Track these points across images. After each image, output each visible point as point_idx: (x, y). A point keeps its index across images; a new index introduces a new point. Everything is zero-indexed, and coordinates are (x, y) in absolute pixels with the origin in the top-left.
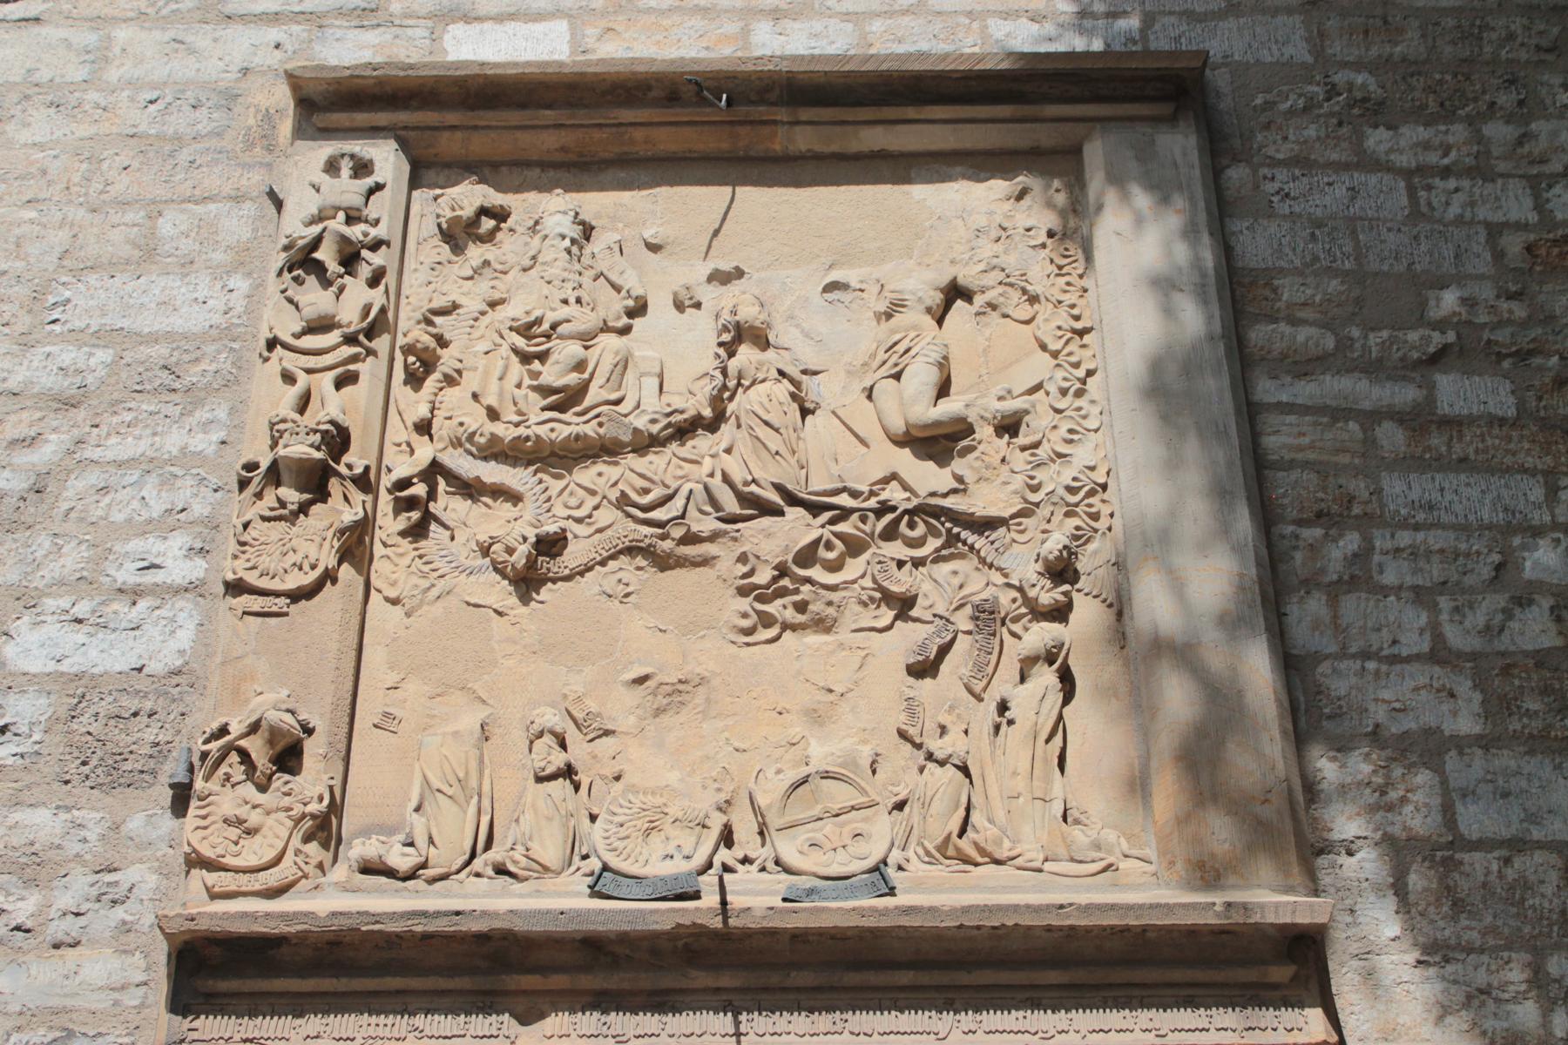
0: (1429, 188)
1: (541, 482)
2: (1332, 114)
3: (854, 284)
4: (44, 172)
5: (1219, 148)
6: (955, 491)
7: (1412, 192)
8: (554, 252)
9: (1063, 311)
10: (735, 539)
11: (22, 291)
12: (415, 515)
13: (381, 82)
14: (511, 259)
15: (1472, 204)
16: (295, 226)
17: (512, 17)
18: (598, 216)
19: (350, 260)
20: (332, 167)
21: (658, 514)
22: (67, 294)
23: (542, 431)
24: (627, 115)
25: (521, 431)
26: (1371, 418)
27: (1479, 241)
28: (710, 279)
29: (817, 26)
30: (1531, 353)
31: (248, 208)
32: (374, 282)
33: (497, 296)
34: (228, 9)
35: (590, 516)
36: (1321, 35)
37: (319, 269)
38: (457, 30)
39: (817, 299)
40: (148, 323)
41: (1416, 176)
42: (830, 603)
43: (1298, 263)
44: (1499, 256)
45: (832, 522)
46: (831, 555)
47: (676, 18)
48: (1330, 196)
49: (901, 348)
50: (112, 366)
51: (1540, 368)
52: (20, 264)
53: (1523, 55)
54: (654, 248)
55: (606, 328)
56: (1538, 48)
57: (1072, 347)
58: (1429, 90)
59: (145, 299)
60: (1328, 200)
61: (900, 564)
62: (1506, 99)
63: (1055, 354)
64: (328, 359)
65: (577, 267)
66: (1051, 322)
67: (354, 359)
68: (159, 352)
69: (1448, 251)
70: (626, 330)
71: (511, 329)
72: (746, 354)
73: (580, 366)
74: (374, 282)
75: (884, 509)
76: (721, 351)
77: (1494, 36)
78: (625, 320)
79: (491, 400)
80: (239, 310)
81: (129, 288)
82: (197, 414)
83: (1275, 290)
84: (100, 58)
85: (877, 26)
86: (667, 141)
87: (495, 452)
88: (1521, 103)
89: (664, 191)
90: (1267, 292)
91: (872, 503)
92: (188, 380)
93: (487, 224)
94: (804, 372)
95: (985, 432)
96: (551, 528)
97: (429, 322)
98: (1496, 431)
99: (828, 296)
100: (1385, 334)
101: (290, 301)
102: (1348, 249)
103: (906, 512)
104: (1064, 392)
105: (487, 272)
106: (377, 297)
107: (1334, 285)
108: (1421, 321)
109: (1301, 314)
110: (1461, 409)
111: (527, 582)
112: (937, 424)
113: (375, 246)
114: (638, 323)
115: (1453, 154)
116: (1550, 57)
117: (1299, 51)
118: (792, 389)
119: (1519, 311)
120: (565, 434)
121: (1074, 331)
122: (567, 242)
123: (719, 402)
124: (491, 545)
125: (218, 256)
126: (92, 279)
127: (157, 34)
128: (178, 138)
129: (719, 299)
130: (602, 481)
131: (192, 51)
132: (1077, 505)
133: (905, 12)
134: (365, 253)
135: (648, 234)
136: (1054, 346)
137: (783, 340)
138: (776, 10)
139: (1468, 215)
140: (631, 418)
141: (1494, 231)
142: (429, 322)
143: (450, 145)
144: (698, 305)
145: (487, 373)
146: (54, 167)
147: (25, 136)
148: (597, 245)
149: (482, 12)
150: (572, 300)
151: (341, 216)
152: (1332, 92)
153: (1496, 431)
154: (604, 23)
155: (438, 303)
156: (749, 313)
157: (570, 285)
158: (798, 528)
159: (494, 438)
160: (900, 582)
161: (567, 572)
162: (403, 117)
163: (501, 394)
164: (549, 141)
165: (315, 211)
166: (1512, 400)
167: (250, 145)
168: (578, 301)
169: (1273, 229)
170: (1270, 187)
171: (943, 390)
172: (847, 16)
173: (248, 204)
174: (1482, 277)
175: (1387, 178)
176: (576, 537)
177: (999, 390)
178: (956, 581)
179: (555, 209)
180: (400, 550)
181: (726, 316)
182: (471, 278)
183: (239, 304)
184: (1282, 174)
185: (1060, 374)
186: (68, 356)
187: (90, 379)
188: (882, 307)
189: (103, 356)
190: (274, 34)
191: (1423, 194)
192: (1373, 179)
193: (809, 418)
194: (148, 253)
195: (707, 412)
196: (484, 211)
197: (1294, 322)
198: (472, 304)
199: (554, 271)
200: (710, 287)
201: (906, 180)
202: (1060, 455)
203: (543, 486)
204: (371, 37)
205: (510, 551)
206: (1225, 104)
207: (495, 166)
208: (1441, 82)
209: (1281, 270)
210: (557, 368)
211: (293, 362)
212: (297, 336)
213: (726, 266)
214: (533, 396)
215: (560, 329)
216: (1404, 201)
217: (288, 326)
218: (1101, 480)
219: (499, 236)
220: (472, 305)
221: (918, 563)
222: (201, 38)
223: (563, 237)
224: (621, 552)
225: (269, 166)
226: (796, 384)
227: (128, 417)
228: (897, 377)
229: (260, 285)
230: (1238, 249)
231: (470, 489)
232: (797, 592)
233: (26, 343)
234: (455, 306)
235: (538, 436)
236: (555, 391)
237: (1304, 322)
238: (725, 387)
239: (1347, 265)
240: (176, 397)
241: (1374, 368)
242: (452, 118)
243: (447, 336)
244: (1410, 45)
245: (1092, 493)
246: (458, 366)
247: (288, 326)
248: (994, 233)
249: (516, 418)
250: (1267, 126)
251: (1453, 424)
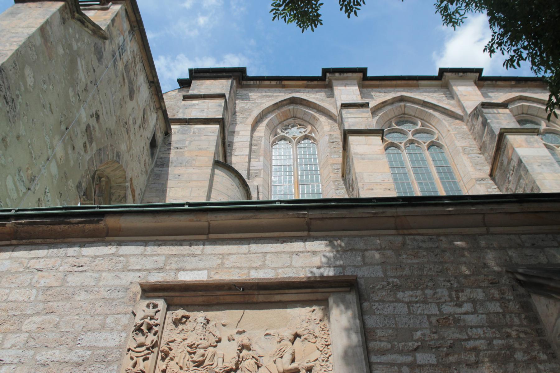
0: (413, 306)
2: (389, 289)
3: (272, 334)
4: (82, 307)
5: (361, 299)
7: (408, 307)
8: (199, 327)
9: (323, 340)
11: (72, 336)
13: (161, 285)
14: (189, 328)
15: (423, 310)
16: (138, 321)
17: (194, 270)
18: (211, 318)
19: (150, 328)
20: (148, 306)
22: (83, 337)
24: (219, 293)
26: (400, 365)
27: (425, 320)
28: (237, 333)
29: (266, 271)
30: (439, 347)
31: (128, 316)
32: (155, 334)
33: (185, 338)
34: (129, 268)
36: (386, 270)
37: (142, 331)
38: (181, 273)
39: (263, 337)
40: (101, 344)
41: (409, 304)
43: (381, 326)
44: (430, 323)
47: (233, 269)
48: (388, 309)
49: (282, 350)
50: (91, 356)
51: (442, 351)
52: (73, 330)
53: (434, 273)
54: (224, 325)
55: (211, 346)
56: (437, 272)
57: (325, 349)
58: (411, 282)
59: (101, 338)
60: (388, 310)
62: (430, 284)
63: (321, 351)
65: (205, 330)
66: (320, 343)
67: (148, 354)
68: (102, 352)
69: (418, 322)
70: (216, 346)
72: (245, 352)
74: (155, 334)
76: (238, 352)
77: (426, 269)
78: (216, 344)
79: (181, 364)
80: (123, 341)
81: (97, 336)
82: (110, 368)
83: (376, 333)
84: (98, 280)
85: (280, 270)
86: (228, 299)
88: (434, 285)
89: (227, 311)
90: (374, 334)
92: (108, 359)
93: (184, 320)
94: (259, 356)
97: (168, 344)
98: (432, 368)
99: (266, 337)
100: (403, 343)
101: (134, 339)
102: (393, 322)
104: (323, 361)
105: (183, 332)
106: (155, 338)
107: (390, 331)
108: (412, 340)
109: (383, 339)
110: (423, 362)
112: (291, 370)
113: (156, 325)
114: (219, 344)
115: (418, 298)
116: (440, 274)
117: (381, 274)
119: (436, 336)
121: (326, 345)
122: (202, 324)
123: (237, 364)
125: (120, 328)
126: (89, 333)
127: (112, 274)
128: (114, 299)
129: (238, 338)
131: (120, 278)
133: (287, 267)
134: (154, 327)
135: (223, 322)
136: (321, 349)
137: (254, 349)
138: (256, 267)
139: (422, 313)
141: (429, 316)
142: (168, 344)
143: (177, 300)
144: (234, 340)
145: (180, 358)
146: (84, 306)
147: (79, 298)
148: (210, 325)
149: (187, 269)
151: (149, 318)
152: (389, 284)
153: (432, 368)
154: (216, 271)
155: (171, 339)
156: (246, 342)
157: (202, 335)
162: (166, 294)
163: (183, 363)
164: (200, 300)
165: (143, 317)
166: (435, 360)
167: (130, 301)
168: (204, 339)
169: (375, 317)
170: (374, 307)
171: (293, 361)
172: (273, 268)
173: (128, 315)
174: (427, 328)
175: (402, 304)
177: (307, 361)
179: (200, 316)
181: (240, 343)
183: (123, 339)
184: (377, 304)
185: (322, 356)
186: (80, 352)
187: (85, 359)
188: (278, 340)
189: (89, 353)
190: (139, 274)
191: (411, 308)
192: (399, 305)
193: (260, 369)
194: (103, 327)
195: (234, 367)
196: (183, 317)
197: (380, 341)
198: (179, 340)
199: (199, 332)
200: (237, 335)
201: (286, 308)
204: (161, 275)
206: (363, 287)
207: (187, 305)
208: (414, 281)
209: (377, 328)
211: (133, 354)
212: (135, 348)
213: (241, 330)
214: (191, 363)
215: (199, 346)
216: (407, 310)
217: (133, 345)
219: (187, 323)
220: (179, 340)
222: (122, 275)
225: (134, 305)
226: (257, 360)
227: (93, 368)
228: (282, 357)
229: (128, 335)
230: (366, 323)
233: (71, 349)
234: (175, 340)
236: (196, 362)
237: (383, 341)
238: (239, 361)
239: (393, 326)
240: (105, 363)
241: (401, 352)
242: (177, 294)
243: (172, 348)
244: (407, 272)
247: (133, 345)
248: (307, 321)
249: (187, 369)
250: (373, 292)
251: (421, 366)
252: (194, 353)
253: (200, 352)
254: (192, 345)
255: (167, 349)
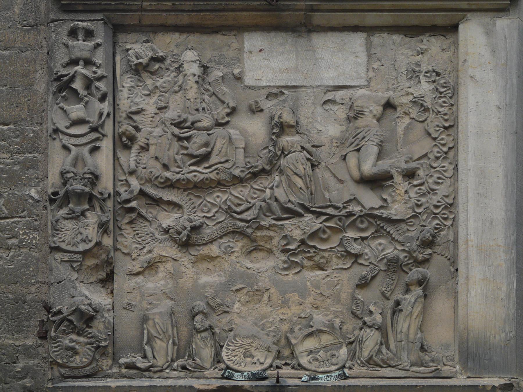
1: (190, 199)
6: (381, 207)
10: (281, 229)
12: (133, 216)
21: (246, 216)
23: (190, 176)
25: (179, 176)
35: (214, 216)
42: (323, 257)
45: (325, 221)
46: (325, 236)
55: (218, 124)
61: (356, 239)
64: (84, 140)
67: (97, 139)
71: (171, 124)
73: (206, 145)
74: (102, 99)
75: (350, 214)
87: (169, 185)
91: (344, 212)
95: (398, 178)
96: (197, 223)
103: (360, 216)
111: (186, 245)
118: (309, 156)
120: (201, 178)
124: (169, 229)
130: (218, 200)
132: (438, 214)
140: (232, 170)
142: (131, 118)
150: (201, 109)
155: (134, 109)
158: (310, 223)
159: (167, 179)
160: (355, 248)
161: (204, 242)
168: (203, 109)
176: (208, 225)
178: (380, 248)
180: (127, 231)
182: (149, 95)
195: (267, 168)
202: (433, 190)
203: (191, 201)
205: (179, 233)
210: (196, 145)
214: (185, 158)
215: (196, 125)
218: (451, 202)
220: (151, 109)
221: (363, 239)
223: (195, 75)
224: (229, 233)
231: (157, 202)
232: (309, 252)
235: (188, 179)
245: (446, 208)
246: (147, 141)
249: (178, 170)
252: (188, 139)
253: (199, 138)
254: (181, 123)
255: (130, 128)
